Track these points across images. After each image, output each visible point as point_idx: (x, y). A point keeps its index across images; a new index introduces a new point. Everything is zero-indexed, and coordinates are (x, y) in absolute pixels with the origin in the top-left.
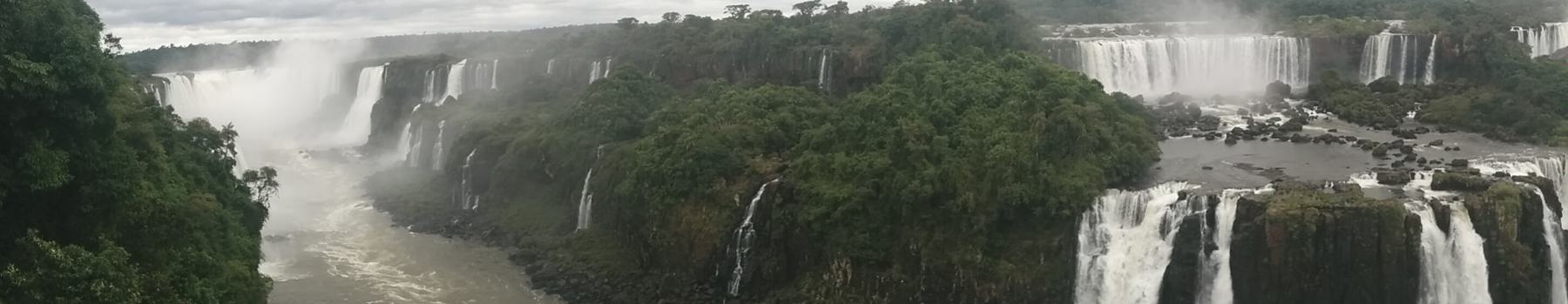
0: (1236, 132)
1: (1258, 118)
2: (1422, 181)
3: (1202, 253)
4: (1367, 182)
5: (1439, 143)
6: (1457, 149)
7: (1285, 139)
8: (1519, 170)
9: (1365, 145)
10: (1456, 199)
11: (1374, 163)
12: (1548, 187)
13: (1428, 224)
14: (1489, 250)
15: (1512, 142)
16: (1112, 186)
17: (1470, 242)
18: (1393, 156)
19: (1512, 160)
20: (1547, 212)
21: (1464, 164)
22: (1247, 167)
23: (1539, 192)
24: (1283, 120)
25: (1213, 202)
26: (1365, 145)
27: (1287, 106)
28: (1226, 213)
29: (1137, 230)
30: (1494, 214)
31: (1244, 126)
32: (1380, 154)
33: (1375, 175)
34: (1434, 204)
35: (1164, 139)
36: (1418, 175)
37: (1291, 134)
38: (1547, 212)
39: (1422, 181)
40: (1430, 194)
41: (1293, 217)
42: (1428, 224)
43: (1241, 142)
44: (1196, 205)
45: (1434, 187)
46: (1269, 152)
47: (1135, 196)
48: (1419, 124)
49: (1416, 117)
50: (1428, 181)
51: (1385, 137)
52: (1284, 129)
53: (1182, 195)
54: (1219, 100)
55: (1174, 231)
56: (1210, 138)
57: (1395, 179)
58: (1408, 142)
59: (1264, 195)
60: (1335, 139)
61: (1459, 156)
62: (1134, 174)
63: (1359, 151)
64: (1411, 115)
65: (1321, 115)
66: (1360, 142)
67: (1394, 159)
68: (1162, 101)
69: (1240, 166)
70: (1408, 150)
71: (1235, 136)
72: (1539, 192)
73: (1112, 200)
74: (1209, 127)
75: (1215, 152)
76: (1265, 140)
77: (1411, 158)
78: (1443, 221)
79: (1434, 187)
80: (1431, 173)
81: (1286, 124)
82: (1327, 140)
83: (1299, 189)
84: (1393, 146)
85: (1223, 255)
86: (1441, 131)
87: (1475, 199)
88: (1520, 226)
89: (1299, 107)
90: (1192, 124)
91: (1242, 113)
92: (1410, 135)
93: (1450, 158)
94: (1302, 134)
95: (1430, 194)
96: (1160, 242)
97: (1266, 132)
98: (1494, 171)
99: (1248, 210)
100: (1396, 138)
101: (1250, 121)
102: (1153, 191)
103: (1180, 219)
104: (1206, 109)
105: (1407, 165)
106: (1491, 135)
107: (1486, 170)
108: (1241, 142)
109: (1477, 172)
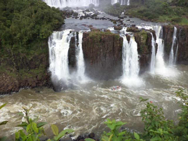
0: (82, 16)
1: (87, 13)
2: (124, 29)
3: (76, 45)
4: (112, 29)
5: (129, 20)
6: (133, 22)
7: (93, 18)
8: (148, 28)
9: (111, 20)
10: (132, 34)
11: (113, 25)
12: (154, 33)
13: (125, 40)
14: (138, 46)
15: (147, 21)
16: (54, 30)
17: (134, 45)
18: (118, 23)
19: (146, 25)
20: (153, 39)
21: (134, 26)
22: (85, 25)
23: (151, 34)
24: (93, 14)
25: (77, 34)
26: (111, 20)
27: (94, 10)
28: (81, 36)
29: (61, 41)
30: (140, 38)
31: (84, 15)
32: (115, 23)
33: (113, 28)
34: (127, 35)
35: (65, 18)
36: (123, 28)
37: (94, 17)
38: (153, 39)
39: (124, 29)
40: (126, 33)
41: (95, 37)
42: (125, 40)
43: (83, 19)
44: (74, 34)
45: (127, 31)
46: (90, 21)
47: (60, 33)
48: (125, 16)
49: (124, 14)
50: (126, 29)
51: (116, 18)
53: (71, 32)
54: (78, 8)
55: (69, 41)
56: (76, 18)
57: (118, 29)
58: (121, 20)
59: (89, 32)
60: (105, 19)
61: (133, 24)
62: (59, 27)
63: (110, 21)
64: (123, 13)
65: (102, 13)
66: (111, 19)
67: (118, 24)
68: (64, 9)
69: (83, 25)
70: (121, 22)
71: (82, 18)
72: (151, 34)
73: (55, 34)
74: (76, 15)
75: (78, 21)
76: (89, 19)
77: (122, 24)
78: (128, 39)
79: (127, 31)
80: (127, 28)
81: (94, 15)
82: (103, 19)
83: (96, 31)
84: (118, 21)
85: (80, 45)
86: (130, 17)
87: (136, 34)
88: (146, 41)
89: (97, 10)
90: (72, 15)
91: (83, 12)
92: (122, 18)
93: (131, 24)
94: (97, 17)
95: (126, 33)
96: (67, 43)
97: (89, 17)
98: (141, 28)
99: (85, 35)
100: (119, 19)
101: (85, 14)
102: (64, 31)
103: (70, 38)
104: (74, 11)
105: (121, 25)
106: (142, 19)
107: (140, 27)
108: (83, 19)
109: (137, 28)
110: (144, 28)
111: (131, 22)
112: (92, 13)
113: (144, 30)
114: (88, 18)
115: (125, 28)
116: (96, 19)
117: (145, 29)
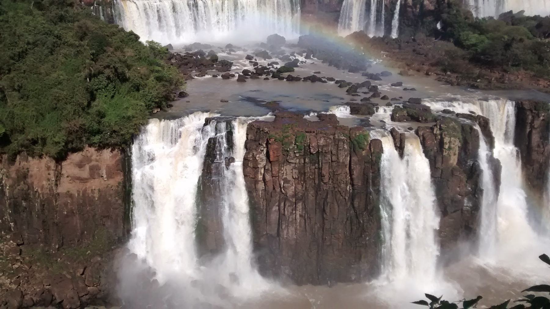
2: (384, 113)
6: (413, 89)
7: (281, 79)
23: (477, 128)
52: (280, 71)
67: (363, 96)
72: (477, 128)
80: (392, 108)
101: (256, 64)
110: (451, 109)
111: (405, 89)
112: (277, 63)
113: (447, 115)
114: (264, 76)
115: (386, 108)
116: (290, 79)
117: (453, 112)
